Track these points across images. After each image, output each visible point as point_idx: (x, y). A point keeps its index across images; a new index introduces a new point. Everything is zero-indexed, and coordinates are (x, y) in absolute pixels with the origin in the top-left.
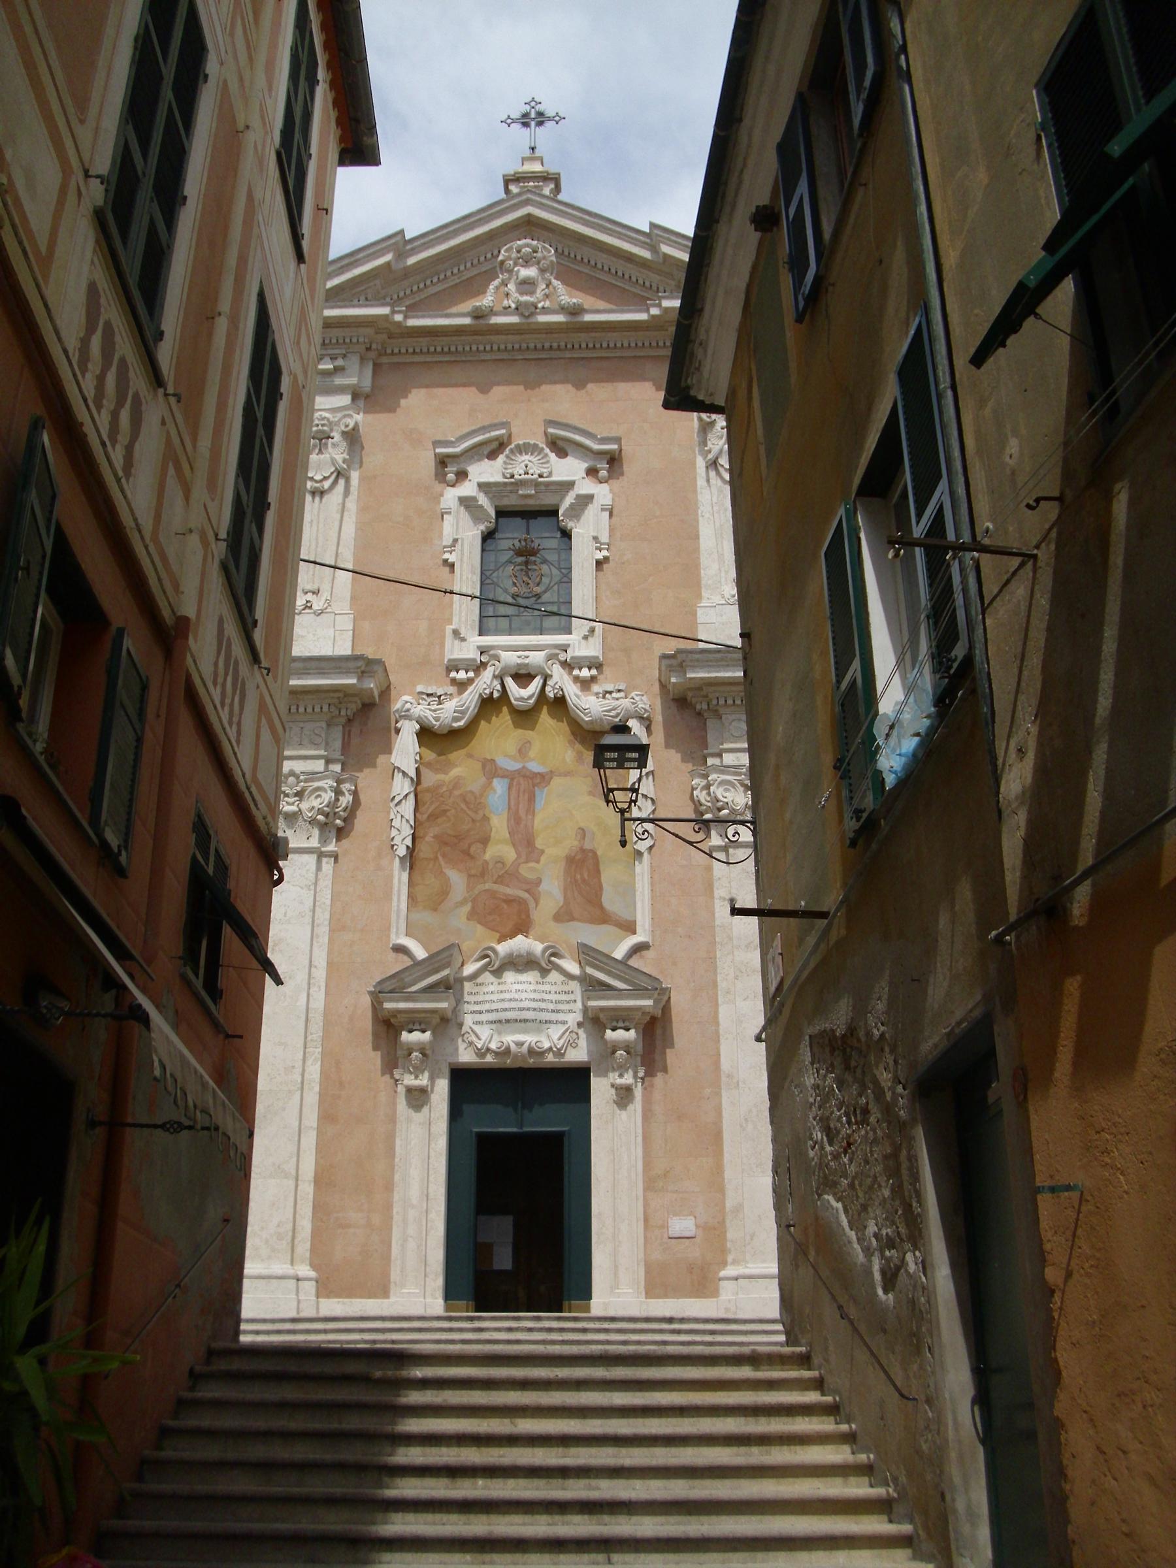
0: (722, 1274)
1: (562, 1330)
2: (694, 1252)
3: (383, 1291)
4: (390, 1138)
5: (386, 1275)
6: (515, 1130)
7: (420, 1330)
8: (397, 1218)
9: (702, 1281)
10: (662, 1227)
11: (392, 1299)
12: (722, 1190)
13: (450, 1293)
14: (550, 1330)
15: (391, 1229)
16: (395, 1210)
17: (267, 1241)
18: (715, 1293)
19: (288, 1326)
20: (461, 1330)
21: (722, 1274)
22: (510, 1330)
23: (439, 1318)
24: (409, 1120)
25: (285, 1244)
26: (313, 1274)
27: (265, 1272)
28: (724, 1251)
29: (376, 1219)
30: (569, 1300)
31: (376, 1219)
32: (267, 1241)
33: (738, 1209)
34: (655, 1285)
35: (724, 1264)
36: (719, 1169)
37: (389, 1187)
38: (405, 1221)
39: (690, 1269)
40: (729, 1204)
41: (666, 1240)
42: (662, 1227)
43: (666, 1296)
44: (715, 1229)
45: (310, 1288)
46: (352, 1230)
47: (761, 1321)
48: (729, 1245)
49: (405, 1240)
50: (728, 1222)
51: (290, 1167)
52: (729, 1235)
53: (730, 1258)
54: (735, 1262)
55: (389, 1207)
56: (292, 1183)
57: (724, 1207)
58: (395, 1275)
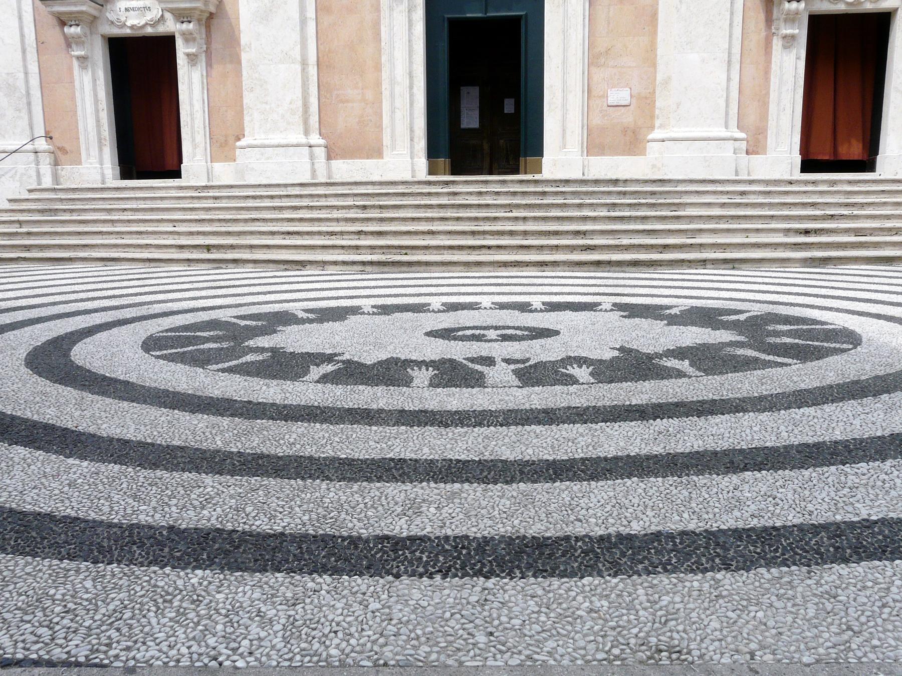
0: (650, 137)
1: (524, 193)
2: (627, 118)
3: (376, 152)
4: (377, 25)
5: (380, 141)
6: (480, 15)
7: (403, 194)
8: (386, 94)
9: (632, 141)
10: (603, 96)
11: (386, 159)
12: (654, 65)
13: (432, 152)
14: (514, 194)
15: (381, 102)
16: (384, 87)
17: (283, 116)
18: (643, 152)
19: (297, 191)
20: (437, 194)
21: (650, 137)
22: (480, 193)
23: (419, 183)
24: (391, 9)
25: (298, 119)
26: (322, 142)
27: (284, 142)
28: (652, 117)
29: (369, 95)
30: (526, 156)
31: (369, 95)
32: (283, 116)
33: (667, 82)
34: (595, 144)
35: (652, 128)
36: (652, 48)
37: (378, 68)
38: (392, 95)
39: (625, 131)
40: (659, 77)
41: (605, 108)
42: (603, 96)
43: (603, 154)
44: (646, 98)
45: (321, 153)
46: (350, 104)
47: (692, 181)
48: (657, 112)
49: (393, 112)
50: (657, 92)
51: (297, 54)
52: (658, 104)
53: (657, 123)
54: (661, 126)
55: (378, 84)
56: (298, 67)
57: (655, 79)
58: (387, 140)
